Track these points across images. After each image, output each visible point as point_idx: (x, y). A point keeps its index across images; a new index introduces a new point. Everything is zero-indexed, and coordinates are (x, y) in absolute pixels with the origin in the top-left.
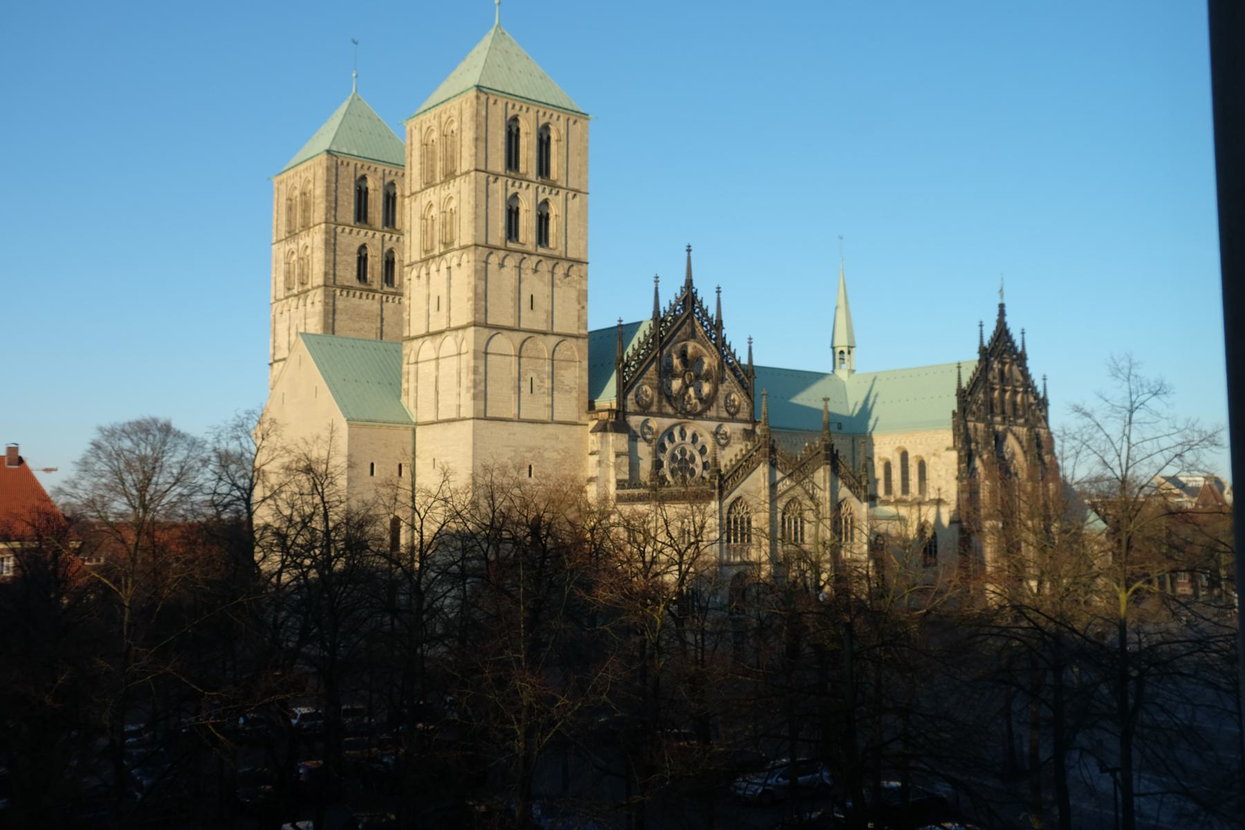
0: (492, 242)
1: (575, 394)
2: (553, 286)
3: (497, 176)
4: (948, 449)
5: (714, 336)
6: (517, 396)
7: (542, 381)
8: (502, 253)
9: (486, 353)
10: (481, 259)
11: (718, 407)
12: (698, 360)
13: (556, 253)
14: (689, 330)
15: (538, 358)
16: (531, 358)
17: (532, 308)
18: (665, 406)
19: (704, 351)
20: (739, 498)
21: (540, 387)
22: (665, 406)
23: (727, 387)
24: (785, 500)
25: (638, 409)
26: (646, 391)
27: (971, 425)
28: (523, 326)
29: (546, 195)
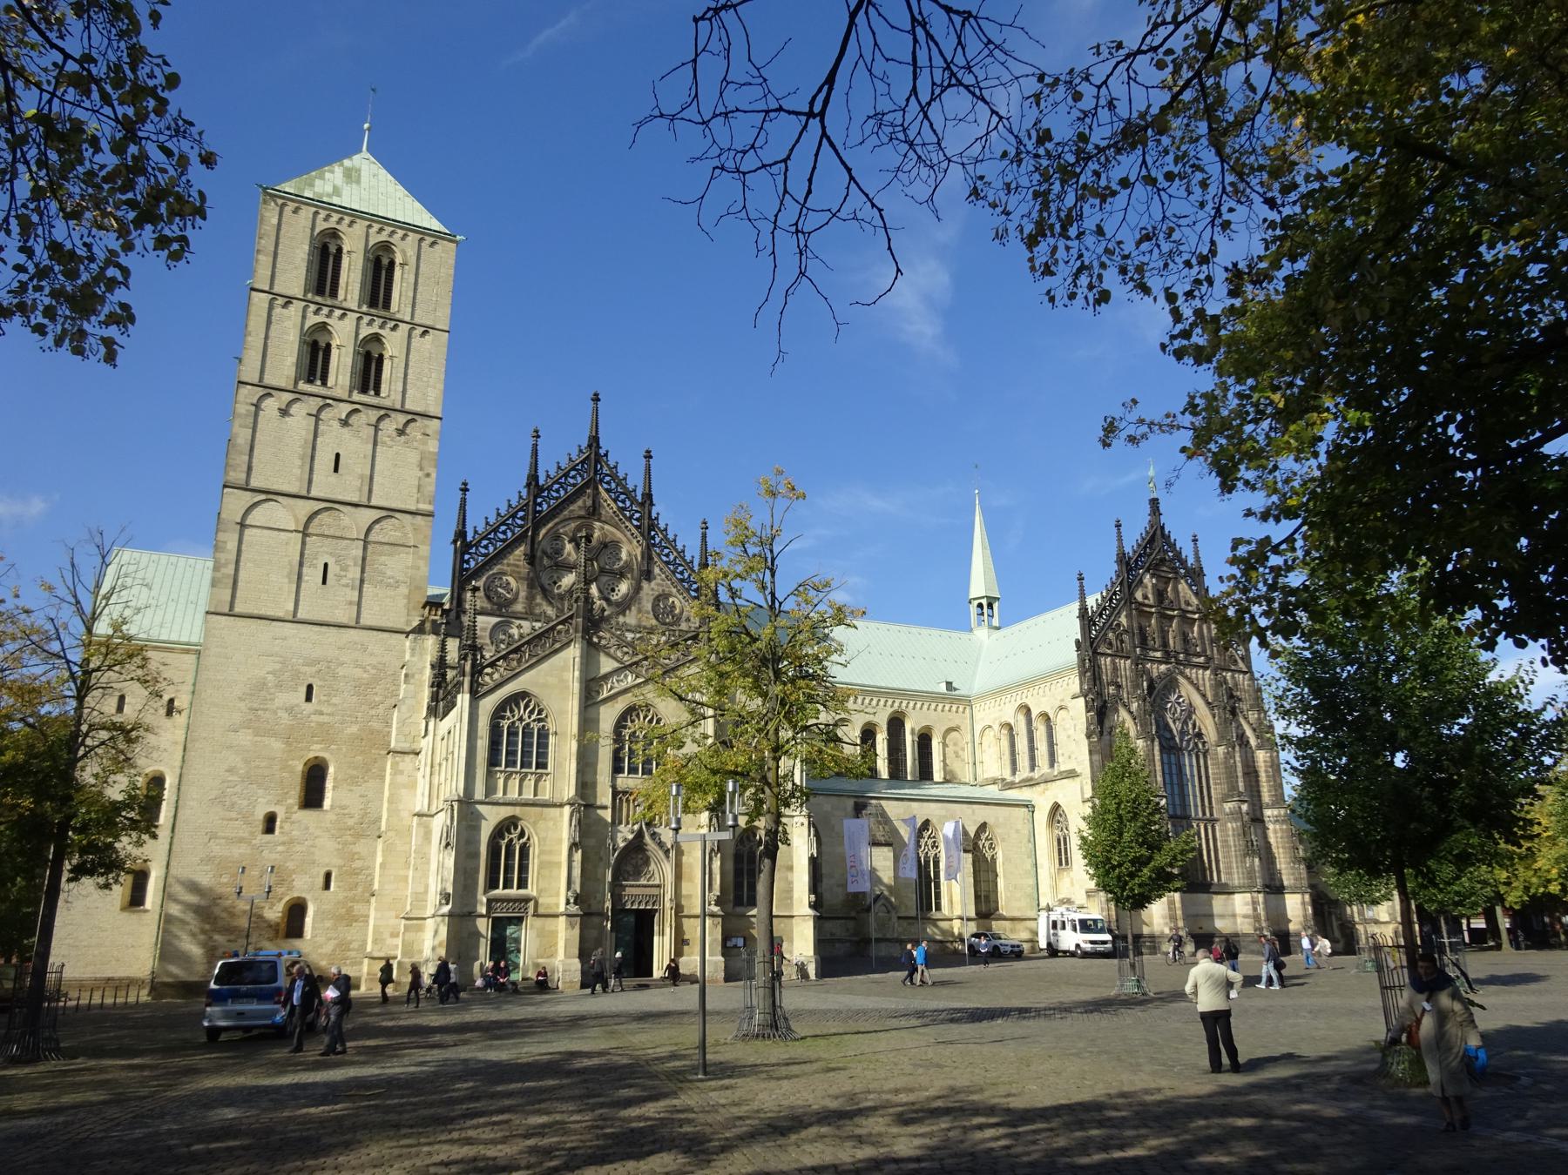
0: (269, 380)
1: (404, 590)
2: (375, 444)
3: (289, 301)
4: (1074, 697)
5: (637, 515)
6: (294, 586)
7: (344, 569)
8: (288, 397)
9: (243, 525)
10: (249, 401)
11: (640, 611)
12: (610, 546)
13: (387, 403)
14: (589, 503)
15: (342, 538)
16: (327, 536)
17: (336, 470)
18: (540, 605)
19: (619, 535)
20: (523, 695)
21: (339, 577)
22: (540, 605)
23: (658, 585)
24: (620, 705)
25: (487, 605)
26: (508, 584)
27: (1106, 662)
28: (313, 493)
29: (375, 329)
